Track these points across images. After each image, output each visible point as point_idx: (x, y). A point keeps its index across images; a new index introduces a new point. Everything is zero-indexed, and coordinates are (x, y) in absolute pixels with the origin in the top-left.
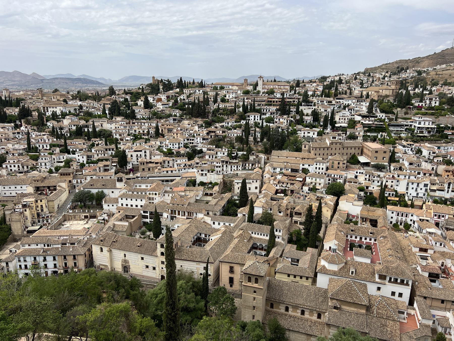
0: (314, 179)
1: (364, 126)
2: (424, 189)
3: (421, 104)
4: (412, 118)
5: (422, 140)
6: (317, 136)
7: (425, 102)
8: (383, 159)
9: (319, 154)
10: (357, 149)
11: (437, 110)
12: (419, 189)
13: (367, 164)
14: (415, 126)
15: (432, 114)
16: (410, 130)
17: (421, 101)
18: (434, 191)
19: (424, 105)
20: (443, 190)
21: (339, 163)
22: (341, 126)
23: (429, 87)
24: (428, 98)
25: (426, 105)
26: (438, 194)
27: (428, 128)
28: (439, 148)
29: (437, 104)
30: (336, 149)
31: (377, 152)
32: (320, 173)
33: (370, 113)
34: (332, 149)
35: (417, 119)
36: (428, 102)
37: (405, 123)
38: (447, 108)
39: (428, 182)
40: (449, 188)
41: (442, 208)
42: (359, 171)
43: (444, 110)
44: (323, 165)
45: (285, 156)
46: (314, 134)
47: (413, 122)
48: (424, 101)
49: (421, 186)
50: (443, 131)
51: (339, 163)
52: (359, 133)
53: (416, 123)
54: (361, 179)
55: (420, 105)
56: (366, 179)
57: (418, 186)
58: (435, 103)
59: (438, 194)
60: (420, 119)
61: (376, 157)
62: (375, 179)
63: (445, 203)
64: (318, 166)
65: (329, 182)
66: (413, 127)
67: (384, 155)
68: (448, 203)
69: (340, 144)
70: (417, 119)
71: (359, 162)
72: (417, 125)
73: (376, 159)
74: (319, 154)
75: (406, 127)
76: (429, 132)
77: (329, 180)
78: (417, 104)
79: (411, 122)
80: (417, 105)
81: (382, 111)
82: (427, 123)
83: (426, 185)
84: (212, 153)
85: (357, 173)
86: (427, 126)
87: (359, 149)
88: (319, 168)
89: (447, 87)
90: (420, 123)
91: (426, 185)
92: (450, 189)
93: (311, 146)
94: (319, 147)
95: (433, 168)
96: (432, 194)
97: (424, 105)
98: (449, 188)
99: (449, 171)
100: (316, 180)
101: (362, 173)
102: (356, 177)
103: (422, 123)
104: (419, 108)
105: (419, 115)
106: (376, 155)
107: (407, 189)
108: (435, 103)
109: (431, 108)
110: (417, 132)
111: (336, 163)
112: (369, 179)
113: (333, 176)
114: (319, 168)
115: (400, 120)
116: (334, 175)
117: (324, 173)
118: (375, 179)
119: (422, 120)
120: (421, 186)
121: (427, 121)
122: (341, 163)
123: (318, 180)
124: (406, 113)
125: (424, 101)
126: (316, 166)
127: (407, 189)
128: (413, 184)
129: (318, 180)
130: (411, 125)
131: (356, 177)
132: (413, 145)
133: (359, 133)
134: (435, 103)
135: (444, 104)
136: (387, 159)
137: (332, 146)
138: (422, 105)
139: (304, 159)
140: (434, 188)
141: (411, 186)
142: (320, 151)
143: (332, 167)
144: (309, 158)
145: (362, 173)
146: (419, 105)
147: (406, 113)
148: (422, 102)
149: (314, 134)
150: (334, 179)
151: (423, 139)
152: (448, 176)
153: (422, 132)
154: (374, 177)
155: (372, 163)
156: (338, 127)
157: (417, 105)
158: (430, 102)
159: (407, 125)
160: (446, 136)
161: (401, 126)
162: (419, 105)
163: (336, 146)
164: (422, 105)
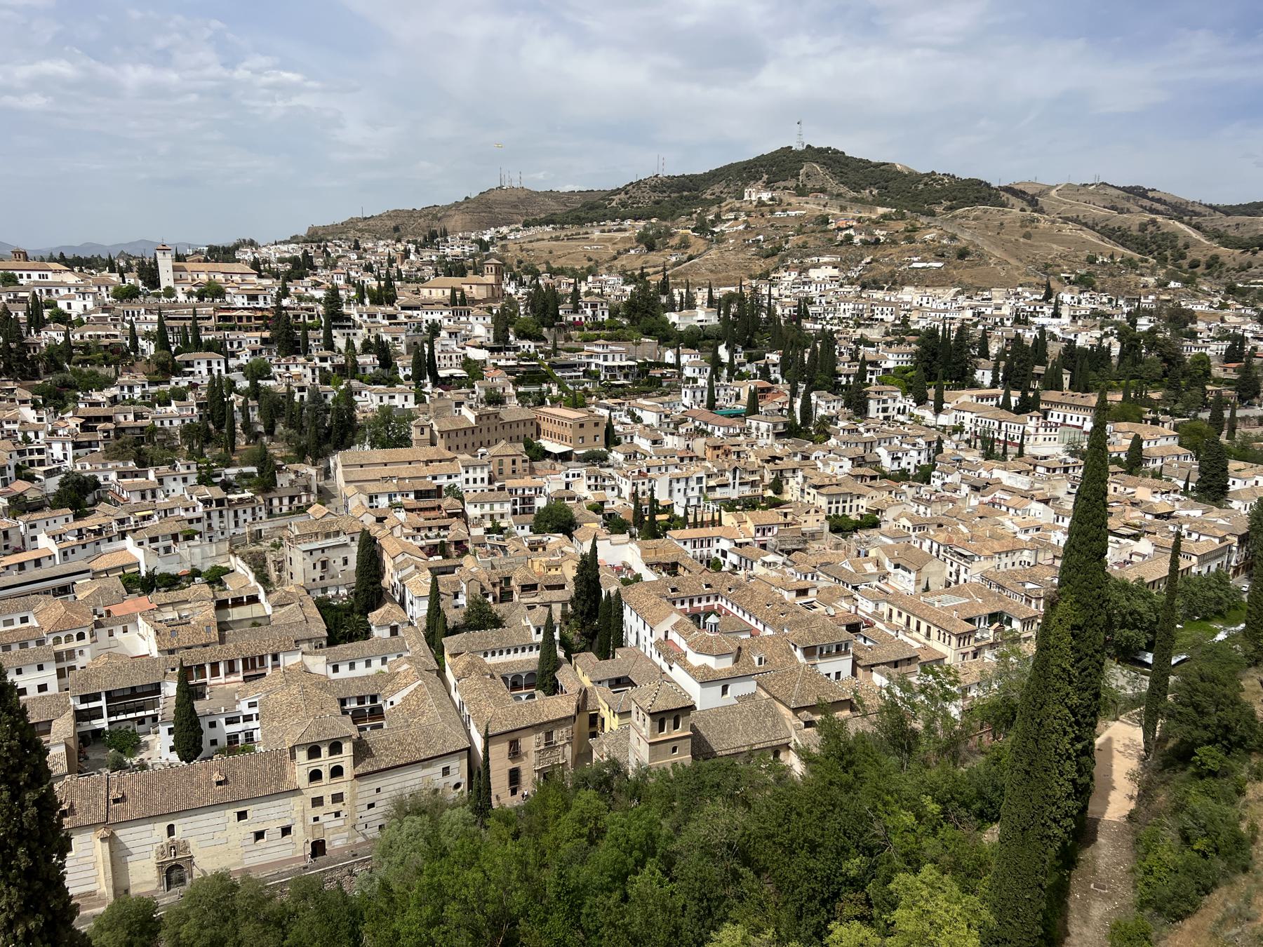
1: (509, 370)
4: (586, 348)
6: (416, 404)
7: (584, 312)
10: (528, 424)
13: (565, 457)
14: (597, 365)
17: (575, 311)
19: (583, 320)
22: (452, 376)
25: (586, 318)
27: (623, 367)
29: (606, 317)
31: (582, 426)
32: (479, 491)
33: (499, 345)
35: (599, 350)
36: (589, 312)
37: (576, 359)
38: (628, 325)
42: (571, 472)
43: (622, 327)
44: (482, 472)
45: (379, 461)
46: (406, 400)
50: (648, 372)
52: (504, 389)
55: (577, 319)
56: (589, 487)
58: (603, 314)
64: (471, 475)
66: (593, 368)
70: (599, 350)
71: (547, 454)
72: (601, 362)
75: (581, 369)
78: (570, 318)
79: (588, 357)
81: (522, 335)
82: (618, 357)
84: (140, 484)
85: (567, 476)
86: (617, 363)
87: (532, 424)
88: (475, 481)
90: (605, 359)
93: (435, 428)
97: (583, 320)
100: (492, 508)
101: (579, 475)
103: (610, 357)
105: (602, 342)
106: (582, 432)
110: (606, 376)
111: (508, 461)
112: (596, 486)
113: (520, 492)
116: (524, 490)
117: (486, 491)
121: (617, 352)
122: (519, 460)
125: (580, 311)
126: (467, 476)
129: (497, 507)
130: (589, 364)
132: (624, 404)
133: (504, 389)
134: (603, 314)
136: (601, 440)
138: (580, 319)
139: (431, 462)
142: (459, 439)
143: (501, 473)
145: (579, 475)
148: (577, 312)
149: (406, 400)
150: (524, 499)
154: (604, 481)
155: (577, 452)
156: (446, 378)
158: (594, 312)
161: (571, 366)
164: (580, 319)
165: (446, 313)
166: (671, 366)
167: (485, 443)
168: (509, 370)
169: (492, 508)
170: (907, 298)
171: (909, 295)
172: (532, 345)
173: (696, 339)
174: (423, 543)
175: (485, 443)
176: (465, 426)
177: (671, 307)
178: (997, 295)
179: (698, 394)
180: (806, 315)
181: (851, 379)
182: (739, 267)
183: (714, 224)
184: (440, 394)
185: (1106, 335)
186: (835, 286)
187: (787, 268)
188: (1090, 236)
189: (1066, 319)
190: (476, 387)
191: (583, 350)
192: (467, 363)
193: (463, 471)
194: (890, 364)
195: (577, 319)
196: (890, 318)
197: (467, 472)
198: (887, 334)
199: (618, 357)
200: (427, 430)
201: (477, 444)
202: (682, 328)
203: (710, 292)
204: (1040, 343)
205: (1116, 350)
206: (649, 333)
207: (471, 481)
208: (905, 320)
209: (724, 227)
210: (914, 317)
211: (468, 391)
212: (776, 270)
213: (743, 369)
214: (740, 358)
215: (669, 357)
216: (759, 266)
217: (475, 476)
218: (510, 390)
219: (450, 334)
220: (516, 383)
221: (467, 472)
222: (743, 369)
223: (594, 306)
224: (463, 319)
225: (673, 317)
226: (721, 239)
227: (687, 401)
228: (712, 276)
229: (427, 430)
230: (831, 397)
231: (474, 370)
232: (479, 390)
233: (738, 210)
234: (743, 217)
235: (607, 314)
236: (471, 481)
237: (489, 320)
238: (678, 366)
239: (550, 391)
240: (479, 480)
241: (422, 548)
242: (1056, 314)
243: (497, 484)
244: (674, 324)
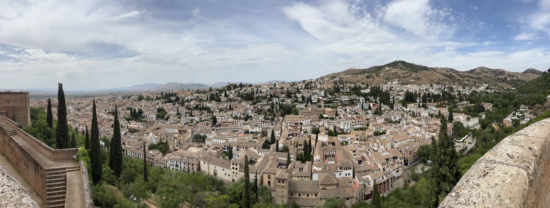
2: (350, 125)
3: (343, 91)
5: (346, 105)
11: (349, 93)
12: (348, 126)
15: (348, 95)
16: (341, 102)
17: (343, 90)
18: (354, 125)
20: (357, 125)
21: (316, 119)
23: (345, 84)
26: (355, 126)
27: (347, 100)
28: (352, 108)
29: (349, 91)
31: (330, 112)
35: (343, 97)
36: (346, 90)
37: (339, 99)
39: (351, 122)
40: (358, 123)
41: (357, 132)
47: (341, 98)
49: (349, 124)
50: (353, 101)
51: (316, 119)
54: (326, 125)
57: (348, 124)
59: (355, 126)
61: (330, 114)
62: (331, 124)
63: (358, 130)
67: (333, 113)
68: (359, 129)
70: (343, 97)
72: (344, 100)
76: (348, 102)
78: (342, 91)
82: (347, 98)
83: (350, 124)
89: (351, 84)
90: (344, 99)
91: (350, 124)
92: (359, 124)
96: (353, 127)
98: (358, 123)
102: (324, 124)
103: (345, 98)
104: (343, 92)
107: (344, 126)
108: (348, 91)
109: (347, 92)
113: (314, 125)
115: (337, 98)
118: (331, 124)
120: (349, 124)
124: (339, 95)
127: (344, 126)
128: (346, 124)
129: (307, 127)
130: (341, 100)
131: (324, 124)
135: (351, 90)
136: (335, 115)
140: (353, 124)
141: (345, 125)
147: (339, 95)
151: (346, 105)
153: (345, 102)
155: (329, 117)
159: (340, 100)
160: (354, 103)
161: (338, 100)
166: (358, 100)
170: (409, 86)
171: (409, 86)
173: (365, 95)
178: (423, 86)
180: (391, 90)
181: (392, 102)
182: (381, 81)
183: (379, 74)
185: (440, 92)
186: (397, 84)
187: (389, 81)
188: (441, 76)
189: (434, 90)
194: (401, 99)
196: (405, 90)
198: (405, 93)
199: (347, 98)
202: (363, 93)
203: (371, 86)
204: (429, 94)
205: (441, 95)
206: (355, 94)
208: (408, 90)
209: (380, 74)
210: (409, 90)
212: (387, 82)
213: (373, 101)
216: (385, 81)
222: (373, 101)
226: (380, 76)
227: (358, 107)
228: (377, 83)
230: (387, 106)
233: (384, 71)
234: (384, 72)
235: (349, 90)
238: (359, 100)
242: (432, 89)
244: (362, 92)
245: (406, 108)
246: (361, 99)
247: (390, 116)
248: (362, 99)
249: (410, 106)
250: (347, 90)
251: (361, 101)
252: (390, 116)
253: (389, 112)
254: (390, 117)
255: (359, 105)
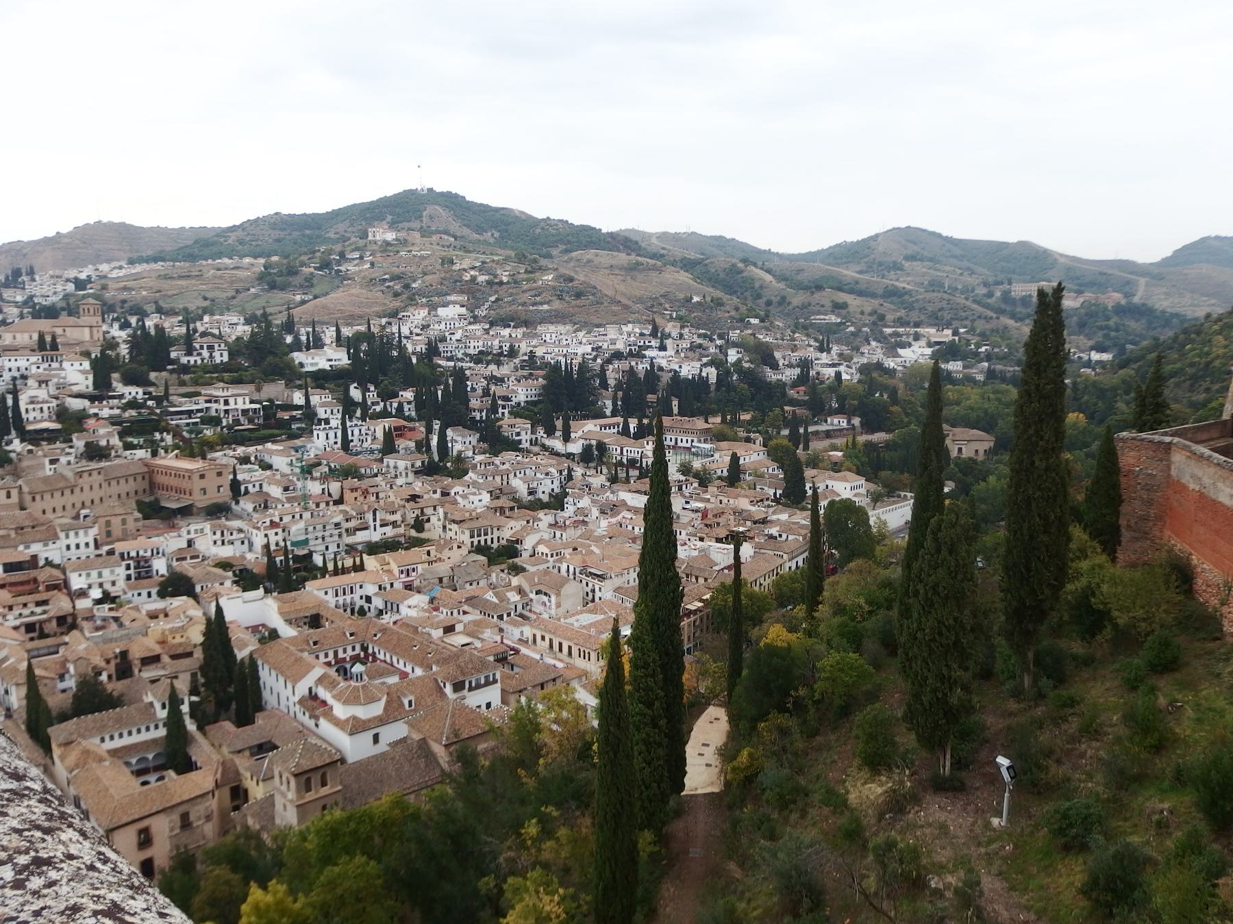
0: (94, 574)
4: (203, 392)
7: (199, 354)
8: (219, 491)
9: (54, 510)
19: (199, 362)
24: (205, 345)
25: (203, 360)
29: (226, 358)
30: (91, 487)
34: (82, 489)
37: (195, 407)
48: (195, 353)
53: (216, 402)
60: (226, 394)
65: (129, 572)
69: (99, 473)
70: (219, 393)
73: (205, 494)
74: (54, 510)
75: (199, 415)
76: (251, 421)
77: (128, 567)
79: (207, 402)
80: (186, 362)
90: (226, 403)
94: (49, 488)
95: (323, 489)
99: (356, 490)
114: (78, 546)
119: (229, 394)
123: (106, 572)
125: (195, 353)
137: (81, 480)
138: (196, 361)
144: (35, 523)
146: (189, 361)
152: (356, 498)
157: (186, 362)
159: (199, 411)
161: (189, 413)
162: (189, 361)
163: (91, 479)
164: (196, 361)
165: (33, 359)
167: (88, 503)
168: (114, 421)
169: (100, 575)
172: (140, 391)
174: (17, 622)
175: (88, 503)
176: (62, 485)
177: (297, 346)
179: (332, 435)
184: (30, 451)
190: (74, 440)
191: (199, 394)
192: (62, 414)
193: (62, 535)
195: (192, 362)
197: (67, 537)
200: (14, 493)
201: (78, 505)
207: (73, 547)
211: (63, 445)
214: (372, 395)
215: (298, 398)
217: (77, 541)
218: (116, 441)
219: (40, 383)
220: (122, 435)
221: (67, 537)
223: (211, 348)
224: (55, 365)
225: (298, 357)
229: (14, 493)
231: (70, 422)
232: (79, 443)
235: (226, 354)
236: (73, 547)
237: (86, 365)
239: (162, 440)
240: (82, 546)
241: (16, 628)
243: (106, 548)
245: (567, 438)
246: (315, 400)
247: (505, 477)
248: (321, 401)
249: (580, 433)
250: (217, 354)
251: (321, 413)
252: (505, 477)
253: (497, 462)
254: (505, 483)
255: (322, 435)
